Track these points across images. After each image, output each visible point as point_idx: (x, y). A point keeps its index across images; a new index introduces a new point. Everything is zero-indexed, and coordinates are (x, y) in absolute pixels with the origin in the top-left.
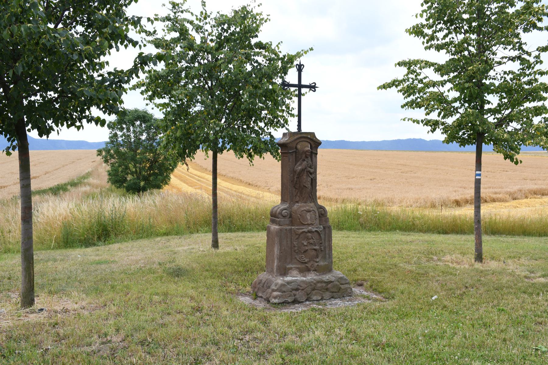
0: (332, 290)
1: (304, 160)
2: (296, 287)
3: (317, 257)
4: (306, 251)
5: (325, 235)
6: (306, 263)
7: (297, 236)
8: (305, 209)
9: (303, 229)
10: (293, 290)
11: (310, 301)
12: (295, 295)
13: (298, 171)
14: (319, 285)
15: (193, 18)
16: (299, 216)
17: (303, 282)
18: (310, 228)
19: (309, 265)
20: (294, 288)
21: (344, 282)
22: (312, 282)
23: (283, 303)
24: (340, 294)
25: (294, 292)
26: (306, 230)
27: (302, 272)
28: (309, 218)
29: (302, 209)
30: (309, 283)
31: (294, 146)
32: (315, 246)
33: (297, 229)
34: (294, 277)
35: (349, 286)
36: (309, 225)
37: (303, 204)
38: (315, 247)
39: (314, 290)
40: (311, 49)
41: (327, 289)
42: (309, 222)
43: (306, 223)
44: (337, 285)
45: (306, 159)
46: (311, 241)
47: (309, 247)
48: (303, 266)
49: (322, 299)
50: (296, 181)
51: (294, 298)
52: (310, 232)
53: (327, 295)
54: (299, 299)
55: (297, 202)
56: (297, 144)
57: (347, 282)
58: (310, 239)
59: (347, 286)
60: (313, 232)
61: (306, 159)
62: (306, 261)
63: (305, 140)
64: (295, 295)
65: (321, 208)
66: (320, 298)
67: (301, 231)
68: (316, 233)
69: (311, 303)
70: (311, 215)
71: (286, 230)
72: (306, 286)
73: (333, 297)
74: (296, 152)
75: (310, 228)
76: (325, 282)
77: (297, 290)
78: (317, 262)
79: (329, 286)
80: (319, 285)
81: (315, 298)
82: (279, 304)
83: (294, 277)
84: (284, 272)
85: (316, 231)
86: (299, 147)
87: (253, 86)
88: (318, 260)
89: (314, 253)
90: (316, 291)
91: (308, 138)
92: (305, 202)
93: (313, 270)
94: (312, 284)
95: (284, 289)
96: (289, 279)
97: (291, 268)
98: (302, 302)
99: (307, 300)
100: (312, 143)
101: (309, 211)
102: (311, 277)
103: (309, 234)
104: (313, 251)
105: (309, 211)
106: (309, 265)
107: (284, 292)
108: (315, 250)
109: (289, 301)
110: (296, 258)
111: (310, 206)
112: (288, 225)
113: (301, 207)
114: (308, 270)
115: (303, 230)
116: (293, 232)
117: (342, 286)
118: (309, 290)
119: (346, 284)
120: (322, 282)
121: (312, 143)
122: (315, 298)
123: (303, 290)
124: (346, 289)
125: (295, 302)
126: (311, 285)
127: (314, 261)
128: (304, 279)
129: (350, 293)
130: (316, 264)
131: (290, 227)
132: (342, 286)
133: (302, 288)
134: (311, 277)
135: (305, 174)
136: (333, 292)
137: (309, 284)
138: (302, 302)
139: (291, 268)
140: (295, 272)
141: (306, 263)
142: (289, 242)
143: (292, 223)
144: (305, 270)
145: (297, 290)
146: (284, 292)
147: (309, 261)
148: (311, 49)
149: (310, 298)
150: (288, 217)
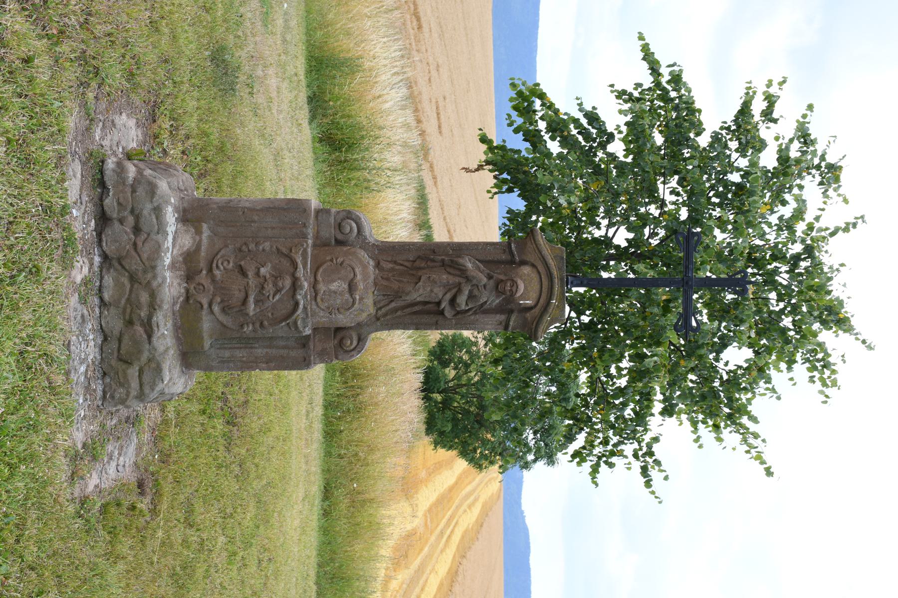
0: (126, 340)
1: (490, 277)
2: (145, 228)
3: (223, 310)
4: (243, 272)
5: (284, 347)
6: (210, 270)
7: (284, 250)
8: (359, 277)
9: (305, 267)
10: (137, 218)
11: (101, 268)
12: (121, 221)
13: (461, 261)
14: (144, 297)
15: (809, 217)
16: (340, 260)
17: (158, 249)
18: (306, 284)
19: (203, 278)
20: (142, 220)
21: (146, 378)
22: (155, 277)
23: (102, 184)
24: (114, 362)
25: (131, 220)
26: (300, 273)
27: (185, 259)
28: (334, 286)
29: (358, 271)
30: (154, 268)
31: (530, 257)
32: (257, 302)
33: (305, 251)
34: (173, 240)
35: (134, 393)
36: (314, 286)
37: (372, 277)
38: (251, 299)
39: (133, 279)
40: (769, 472)
41: (130, 323)
42: (322, 287)
43: (319, 278)
44: (140, 352)
45: (492, 282)
46: (269, 288)
47: (252, 281)
48: (203, 264)
49: (103, 303)
50: (433, 261)
51: (115, 216)
52: (295, 286)
53: (116, 325)
54: (109, 231)
55: (378, 265)
56: (533, 266)
57: (147, 390)
58: (275, 284)
59: (134, 384)
60: (294, 295)
61: (492, 282)
62: (217, 273)
63: (545, 289)
64: (121, 221)
65: (359, 340)
66: (106, 296)
67: (299, 261)
68: (290, 306)
69: (96, 269)
70: (341, 294)
71: (304, 225)
72: (145, 256)
73: (105, 339)
74: (512, 262)
75: (306, 284)
76: (150, 317)
77: (137, 230)
78: (210, 305)
79: (139, 330)
80: (144, 297)
81: (109, 280)
82: (102, 172)
83: (173, 240)
84: (190, 216)
85: (297, 304)
86: (526, 270)
87: (668, 301)
88: (216, 308)
89: (238, 295)
90: (128, 286)
91: (550, 298)
92: (375, 284)
93: (187, 291)
94: (149, 276)
95: (141, 191)
96: (170, 217)
97: (199, 232)
98: (100, 241)
99: (105, 257)
100: (536, 311)
101: (352, 288)
102: (170, 286)
103: (288, 282)
104: (242, 295)
105: (352, 288)
106: (203, 278)
107: (134, 191)
108: (245, 302)
109: (107, 202)
110: (226, 246)
111: (367, 304)
112: (317, 237)
113: (365, 267)
114: (189, 277)
115: (300, 266)
116: (296, 241)
117: (133, 372)
118: (134, 264)
119: (141, 385)
120: (153, 306)
121: (536, 311)
122: (109, 280)
123: (135, 244)
124: (124, 383)
125: (103, 219)
126: (145, 272)
127: (214, 295)
128: (167, 261)
129: (112, 397)
130: (205, 302)
131: (310, 232)
132: (133, 372)
133: (140, 244)
134: (170, 286)
135: (453, 280)
136: (120, 341)
137: (151, 267)
138: (100, 241)
139: (199, 232)
140: (187, 241)
141: (210, 270)
142: (270, 232)
143: (321, 244)
144: (189, 266)
145: (137, 230)
146: (134, 191)
147: (213, 281)
148: (769, 472)
149: (111, 266)
150: (340, 237)
